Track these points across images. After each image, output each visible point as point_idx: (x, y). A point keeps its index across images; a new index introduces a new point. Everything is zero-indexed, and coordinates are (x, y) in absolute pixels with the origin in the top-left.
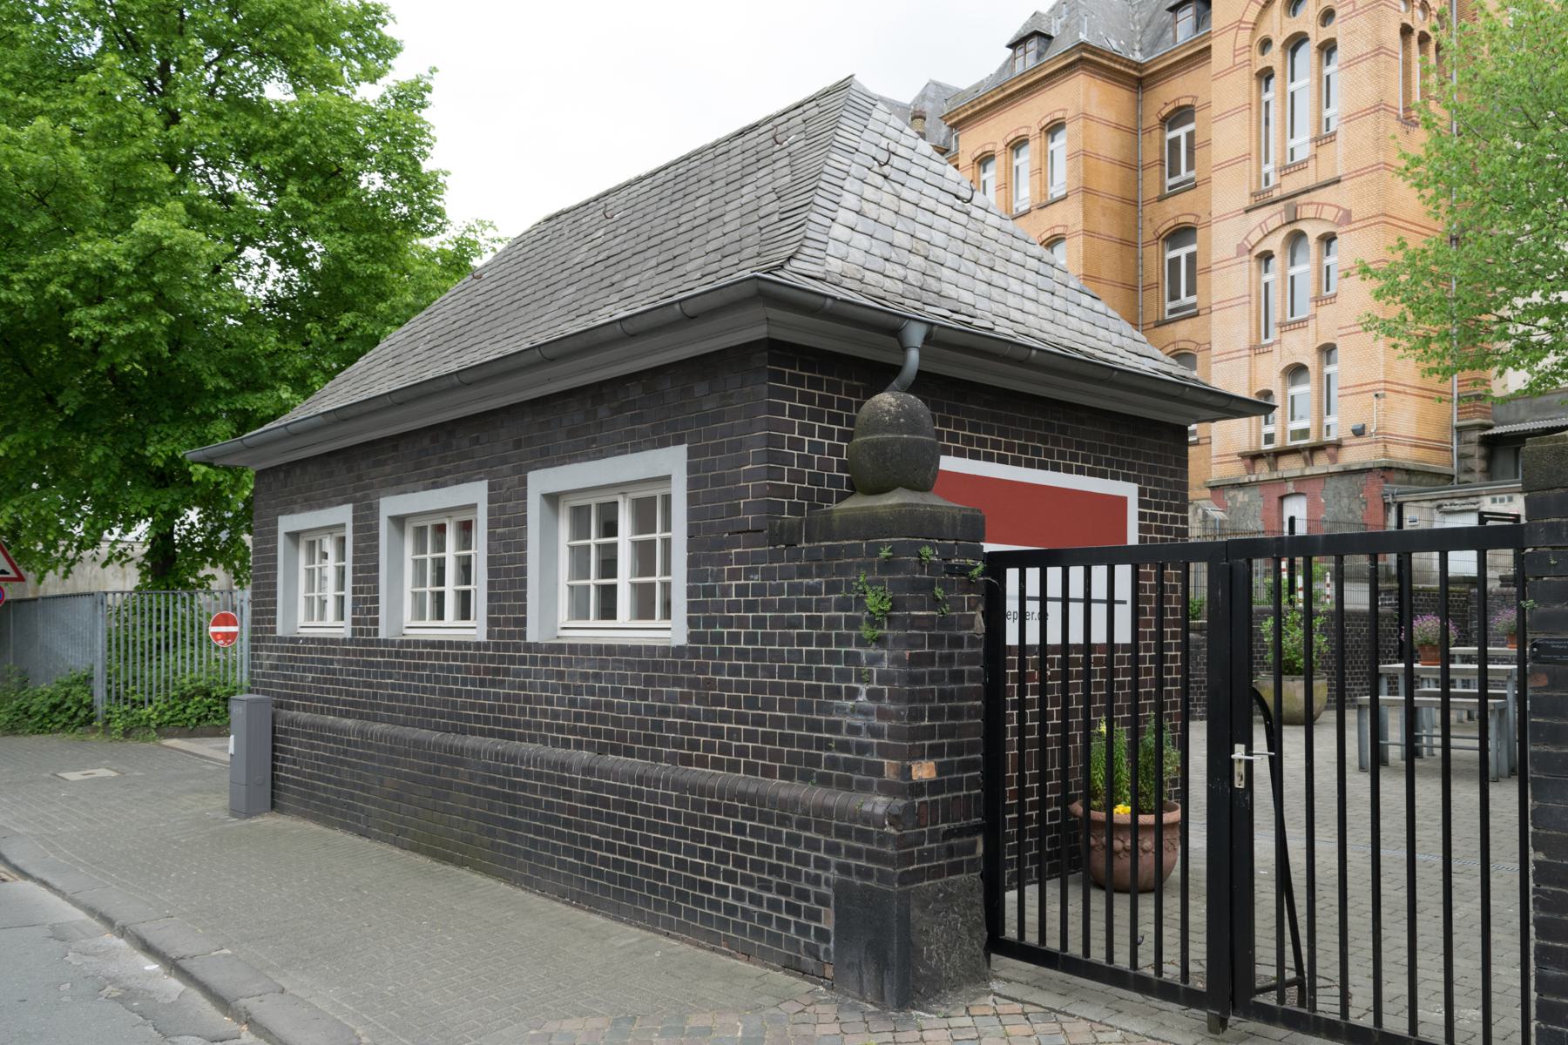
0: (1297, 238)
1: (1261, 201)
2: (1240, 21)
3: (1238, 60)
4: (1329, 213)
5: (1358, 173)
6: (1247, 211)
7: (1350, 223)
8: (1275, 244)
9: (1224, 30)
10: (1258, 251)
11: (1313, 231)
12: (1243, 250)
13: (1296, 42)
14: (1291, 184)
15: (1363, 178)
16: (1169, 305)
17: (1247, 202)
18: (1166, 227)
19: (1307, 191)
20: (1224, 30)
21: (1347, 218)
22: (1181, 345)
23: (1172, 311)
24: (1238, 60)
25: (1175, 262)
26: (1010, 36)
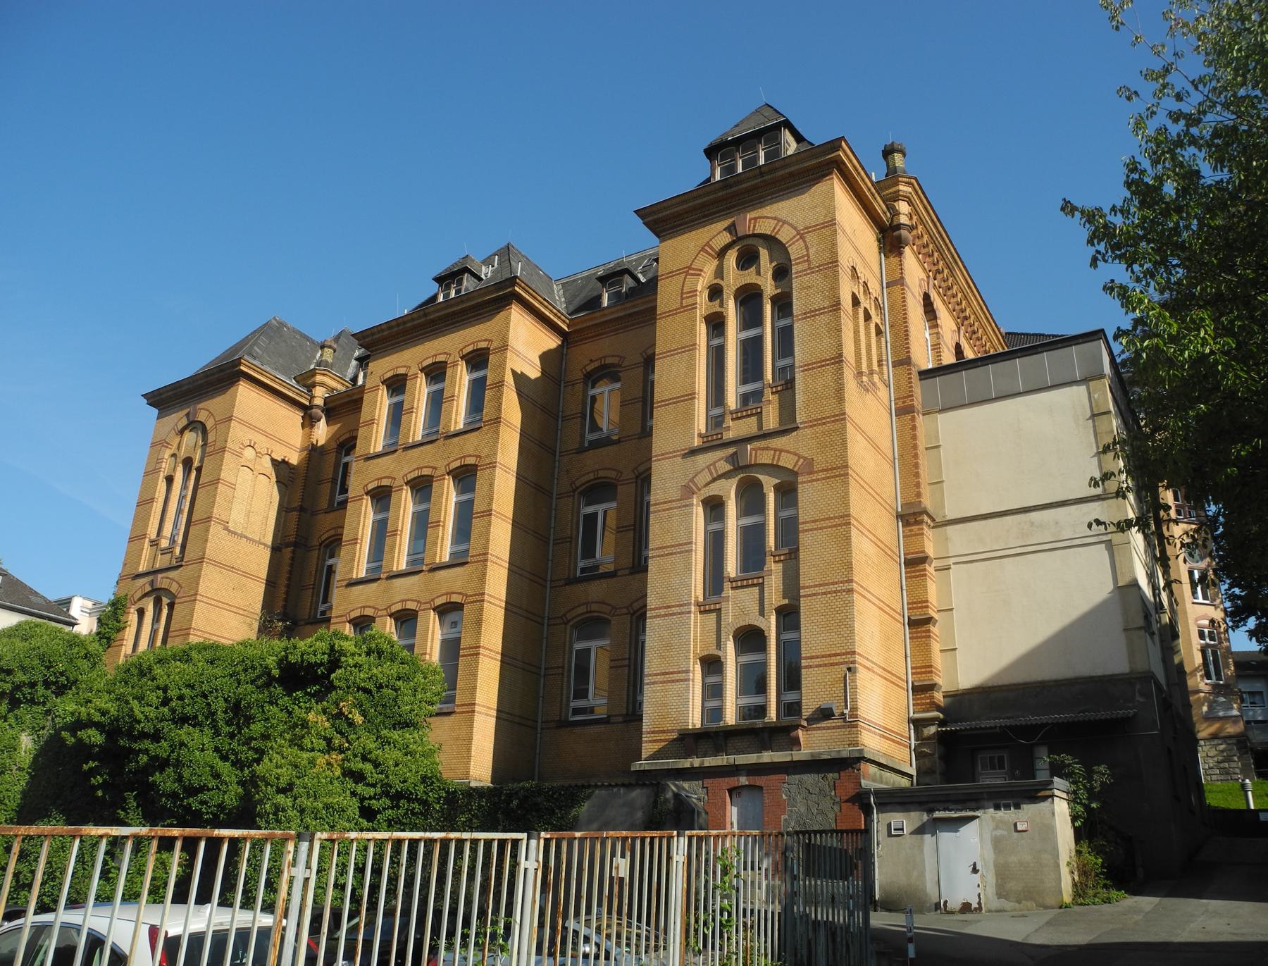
2: (689, 268)
7: (812, 472)
9: (671, 274)
15: (826, 427)
16: (581, 564)
18: (584, 479)
20: (671, 274)
21: (809, 465)
23: (583, 570)
25: (591, 519)
26: (440, 269)
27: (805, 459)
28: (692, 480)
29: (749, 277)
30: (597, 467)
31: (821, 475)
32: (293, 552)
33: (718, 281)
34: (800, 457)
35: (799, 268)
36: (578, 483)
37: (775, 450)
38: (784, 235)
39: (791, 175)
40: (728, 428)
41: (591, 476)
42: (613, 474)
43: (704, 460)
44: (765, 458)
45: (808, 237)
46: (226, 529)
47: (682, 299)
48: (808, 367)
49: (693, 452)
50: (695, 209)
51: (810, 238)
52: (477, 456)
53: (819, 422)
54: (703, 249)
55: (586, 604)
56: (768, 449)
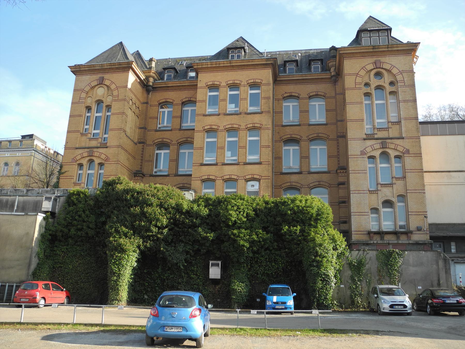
0: (385, 155)
1: (369, 137)
2: (358, 74)
3: (357, 86)
4: (401, 149)
5: (411, 138)
6: (365, 139)
7: (409, 154)
8: (377, 154)
10: (369, 155)
11: (392, 153)
12: (363, 153)
13: (379, 88)
14: (381, 134)
17: (365, 137)
19: (391, 139)
21: (408, 151)
22: (293, 184)
24: (357, 86)
27: (406, 149)
28: (365, 149)
29: (380, 82)
30: (291, 133)
31: (412, 155)
32: (143, 146)
33: (368, 81)
34: (404, 148)
35: (401, 84)
36: (283, 138)
37: (396, 144)
38: (395, 71)
39: (398, 50)
40: (376, 134)
41: (289, 136)
42: (299, 137)
43: (369, 143)
44: (393, 146)
45: (404, 74)
46: (125, 134)
47: (356, 85)
48: (406, 119)
49: (365, 139)
50: (360, 53)
51: (405, 75)
52: (261, 124)
53: (411, 138)
54: (362, 68)
55: (290, 182)
56: (393, 143)
